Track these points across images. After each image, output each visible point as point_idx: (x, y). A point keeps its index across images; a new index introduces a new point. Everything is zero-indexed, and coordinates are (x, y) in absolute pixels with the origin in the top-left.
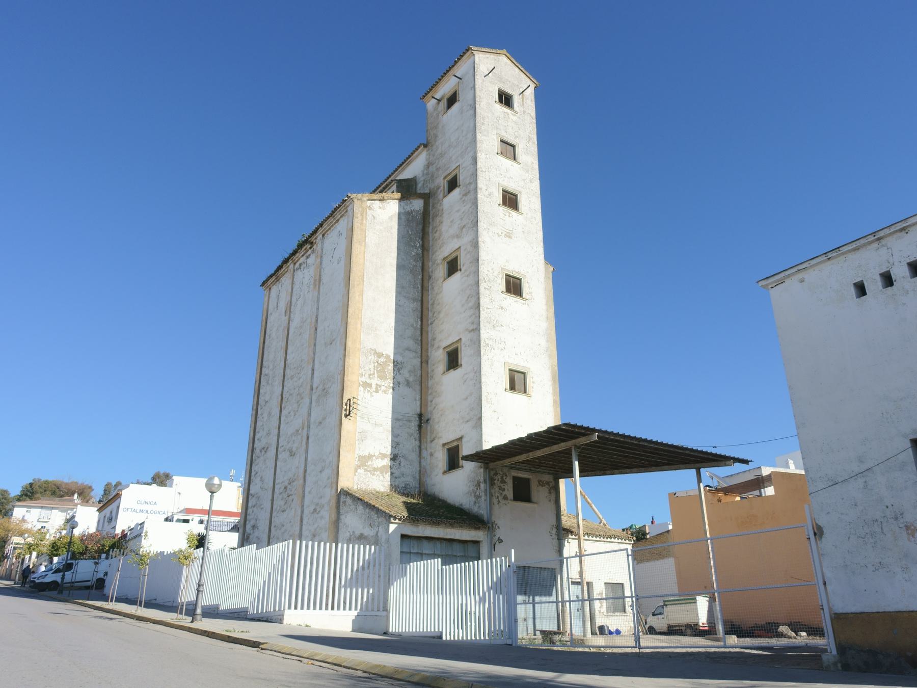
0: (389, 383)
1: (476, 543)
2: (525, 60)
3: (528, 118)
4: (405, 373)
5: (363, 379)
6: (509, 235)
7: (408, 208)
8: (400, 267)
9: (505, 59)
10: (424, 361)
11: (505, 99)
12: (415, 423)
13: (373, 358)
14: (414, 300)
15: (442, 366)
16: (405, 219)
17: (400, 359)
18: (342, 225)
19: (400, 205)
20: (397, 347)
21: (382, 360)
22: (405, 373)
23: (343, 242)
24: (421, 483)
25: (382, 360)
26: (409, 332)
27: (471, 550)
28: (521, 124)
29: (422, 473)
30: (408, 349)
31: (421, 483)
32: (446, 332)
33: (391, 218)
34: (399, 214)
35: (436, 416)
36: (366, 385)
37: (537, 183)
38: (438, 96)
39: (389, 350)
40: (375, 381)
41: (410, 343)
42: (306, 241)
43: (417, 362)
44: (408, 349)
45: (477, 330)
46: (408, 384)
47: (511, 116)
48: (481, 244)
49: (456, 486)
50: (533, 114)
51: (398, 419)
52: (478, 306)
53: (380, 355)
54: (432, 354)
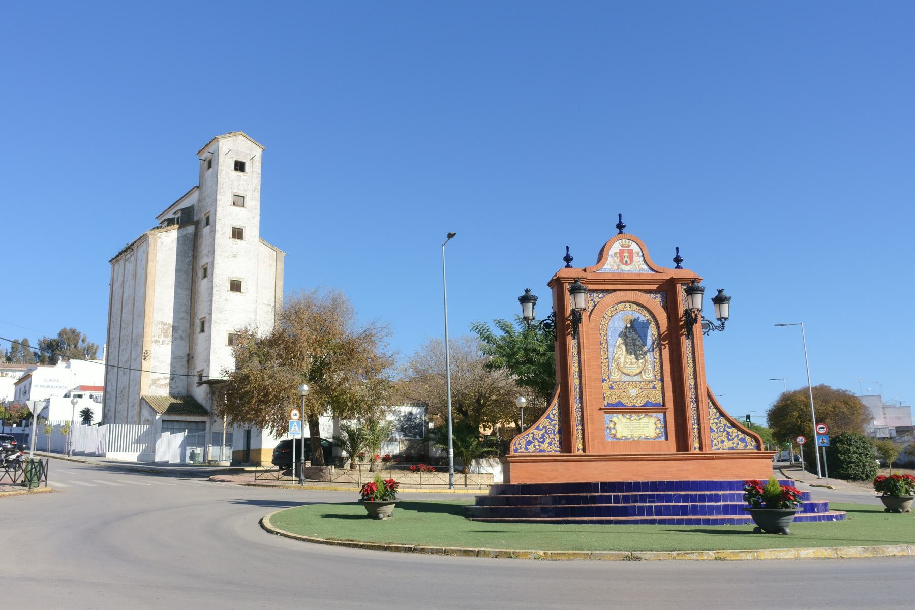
0: (170, 339)
1: (204, 423)
2: (254, 135)
3: (255, 175)
4: (180, 332)
5: (154, 339)
6: (235, 256)
7: (184, 233)
8: (177, 271)
9: (241, 137)
10: (192, 324)
11: (240, 166)
12: (184, 361)
13: (160, 326)
14: (187, 289)
15: (198, 329)
16: (181, 241)
17: (177, 325)
18: (144, 246)
19: (178, 232)
20: (175, 318)
21: (166, 326)
22: (180, 332)
23: (145, 256)
24: (188, 391)
25: (166, 326)
26: (183, 309)
27: (201, 426)
28: (250, 183)
29: (189, 385)
30: (182, 319)
31: (188, 391)
32: (201, 313)
33: (173, 242)
34: (178, 238)
35: (195, 356)
36: (156, 341)
37: (258, 218)
38: (203, 158)
39: (170, 320)
40: (161, 339)
41: (183, 315)
42: (129, 248)
43: (188, 325)
44: (182, 319)
45: (210, 314)
46: (182, 338)
47: (243, 177)
48: (215, 265)
49: (201, 394)
50: (259, 171)
51: (175, 358)
52: (211, 301)
53: (165, 324)
54: (191, 323)
